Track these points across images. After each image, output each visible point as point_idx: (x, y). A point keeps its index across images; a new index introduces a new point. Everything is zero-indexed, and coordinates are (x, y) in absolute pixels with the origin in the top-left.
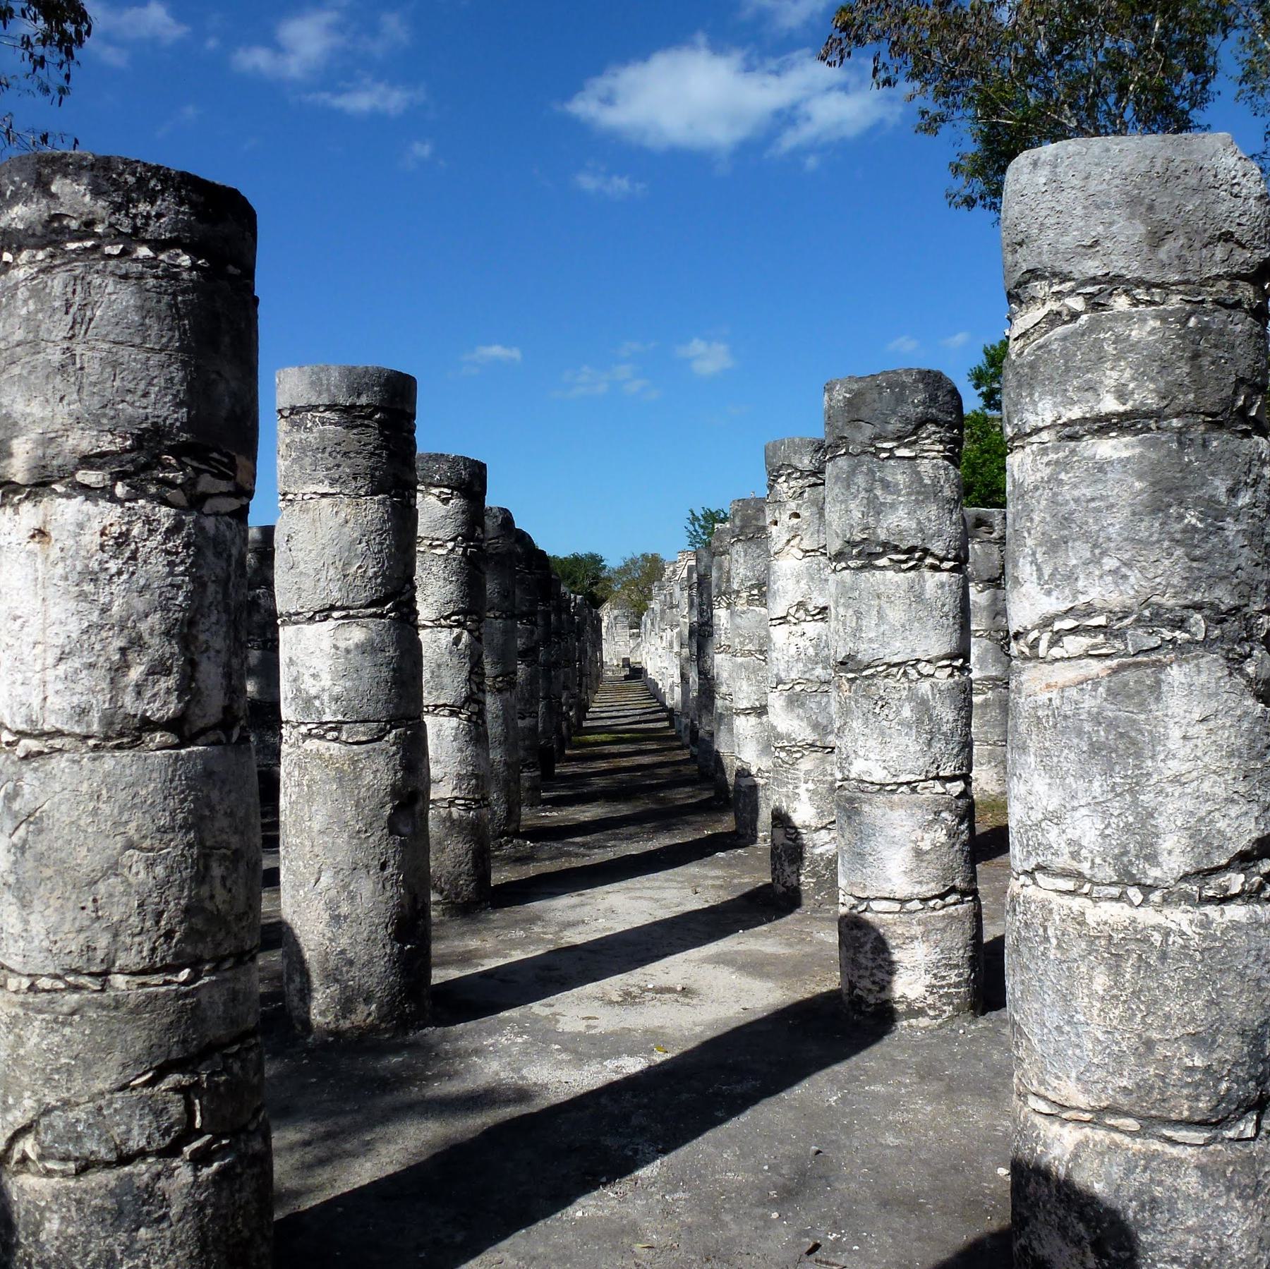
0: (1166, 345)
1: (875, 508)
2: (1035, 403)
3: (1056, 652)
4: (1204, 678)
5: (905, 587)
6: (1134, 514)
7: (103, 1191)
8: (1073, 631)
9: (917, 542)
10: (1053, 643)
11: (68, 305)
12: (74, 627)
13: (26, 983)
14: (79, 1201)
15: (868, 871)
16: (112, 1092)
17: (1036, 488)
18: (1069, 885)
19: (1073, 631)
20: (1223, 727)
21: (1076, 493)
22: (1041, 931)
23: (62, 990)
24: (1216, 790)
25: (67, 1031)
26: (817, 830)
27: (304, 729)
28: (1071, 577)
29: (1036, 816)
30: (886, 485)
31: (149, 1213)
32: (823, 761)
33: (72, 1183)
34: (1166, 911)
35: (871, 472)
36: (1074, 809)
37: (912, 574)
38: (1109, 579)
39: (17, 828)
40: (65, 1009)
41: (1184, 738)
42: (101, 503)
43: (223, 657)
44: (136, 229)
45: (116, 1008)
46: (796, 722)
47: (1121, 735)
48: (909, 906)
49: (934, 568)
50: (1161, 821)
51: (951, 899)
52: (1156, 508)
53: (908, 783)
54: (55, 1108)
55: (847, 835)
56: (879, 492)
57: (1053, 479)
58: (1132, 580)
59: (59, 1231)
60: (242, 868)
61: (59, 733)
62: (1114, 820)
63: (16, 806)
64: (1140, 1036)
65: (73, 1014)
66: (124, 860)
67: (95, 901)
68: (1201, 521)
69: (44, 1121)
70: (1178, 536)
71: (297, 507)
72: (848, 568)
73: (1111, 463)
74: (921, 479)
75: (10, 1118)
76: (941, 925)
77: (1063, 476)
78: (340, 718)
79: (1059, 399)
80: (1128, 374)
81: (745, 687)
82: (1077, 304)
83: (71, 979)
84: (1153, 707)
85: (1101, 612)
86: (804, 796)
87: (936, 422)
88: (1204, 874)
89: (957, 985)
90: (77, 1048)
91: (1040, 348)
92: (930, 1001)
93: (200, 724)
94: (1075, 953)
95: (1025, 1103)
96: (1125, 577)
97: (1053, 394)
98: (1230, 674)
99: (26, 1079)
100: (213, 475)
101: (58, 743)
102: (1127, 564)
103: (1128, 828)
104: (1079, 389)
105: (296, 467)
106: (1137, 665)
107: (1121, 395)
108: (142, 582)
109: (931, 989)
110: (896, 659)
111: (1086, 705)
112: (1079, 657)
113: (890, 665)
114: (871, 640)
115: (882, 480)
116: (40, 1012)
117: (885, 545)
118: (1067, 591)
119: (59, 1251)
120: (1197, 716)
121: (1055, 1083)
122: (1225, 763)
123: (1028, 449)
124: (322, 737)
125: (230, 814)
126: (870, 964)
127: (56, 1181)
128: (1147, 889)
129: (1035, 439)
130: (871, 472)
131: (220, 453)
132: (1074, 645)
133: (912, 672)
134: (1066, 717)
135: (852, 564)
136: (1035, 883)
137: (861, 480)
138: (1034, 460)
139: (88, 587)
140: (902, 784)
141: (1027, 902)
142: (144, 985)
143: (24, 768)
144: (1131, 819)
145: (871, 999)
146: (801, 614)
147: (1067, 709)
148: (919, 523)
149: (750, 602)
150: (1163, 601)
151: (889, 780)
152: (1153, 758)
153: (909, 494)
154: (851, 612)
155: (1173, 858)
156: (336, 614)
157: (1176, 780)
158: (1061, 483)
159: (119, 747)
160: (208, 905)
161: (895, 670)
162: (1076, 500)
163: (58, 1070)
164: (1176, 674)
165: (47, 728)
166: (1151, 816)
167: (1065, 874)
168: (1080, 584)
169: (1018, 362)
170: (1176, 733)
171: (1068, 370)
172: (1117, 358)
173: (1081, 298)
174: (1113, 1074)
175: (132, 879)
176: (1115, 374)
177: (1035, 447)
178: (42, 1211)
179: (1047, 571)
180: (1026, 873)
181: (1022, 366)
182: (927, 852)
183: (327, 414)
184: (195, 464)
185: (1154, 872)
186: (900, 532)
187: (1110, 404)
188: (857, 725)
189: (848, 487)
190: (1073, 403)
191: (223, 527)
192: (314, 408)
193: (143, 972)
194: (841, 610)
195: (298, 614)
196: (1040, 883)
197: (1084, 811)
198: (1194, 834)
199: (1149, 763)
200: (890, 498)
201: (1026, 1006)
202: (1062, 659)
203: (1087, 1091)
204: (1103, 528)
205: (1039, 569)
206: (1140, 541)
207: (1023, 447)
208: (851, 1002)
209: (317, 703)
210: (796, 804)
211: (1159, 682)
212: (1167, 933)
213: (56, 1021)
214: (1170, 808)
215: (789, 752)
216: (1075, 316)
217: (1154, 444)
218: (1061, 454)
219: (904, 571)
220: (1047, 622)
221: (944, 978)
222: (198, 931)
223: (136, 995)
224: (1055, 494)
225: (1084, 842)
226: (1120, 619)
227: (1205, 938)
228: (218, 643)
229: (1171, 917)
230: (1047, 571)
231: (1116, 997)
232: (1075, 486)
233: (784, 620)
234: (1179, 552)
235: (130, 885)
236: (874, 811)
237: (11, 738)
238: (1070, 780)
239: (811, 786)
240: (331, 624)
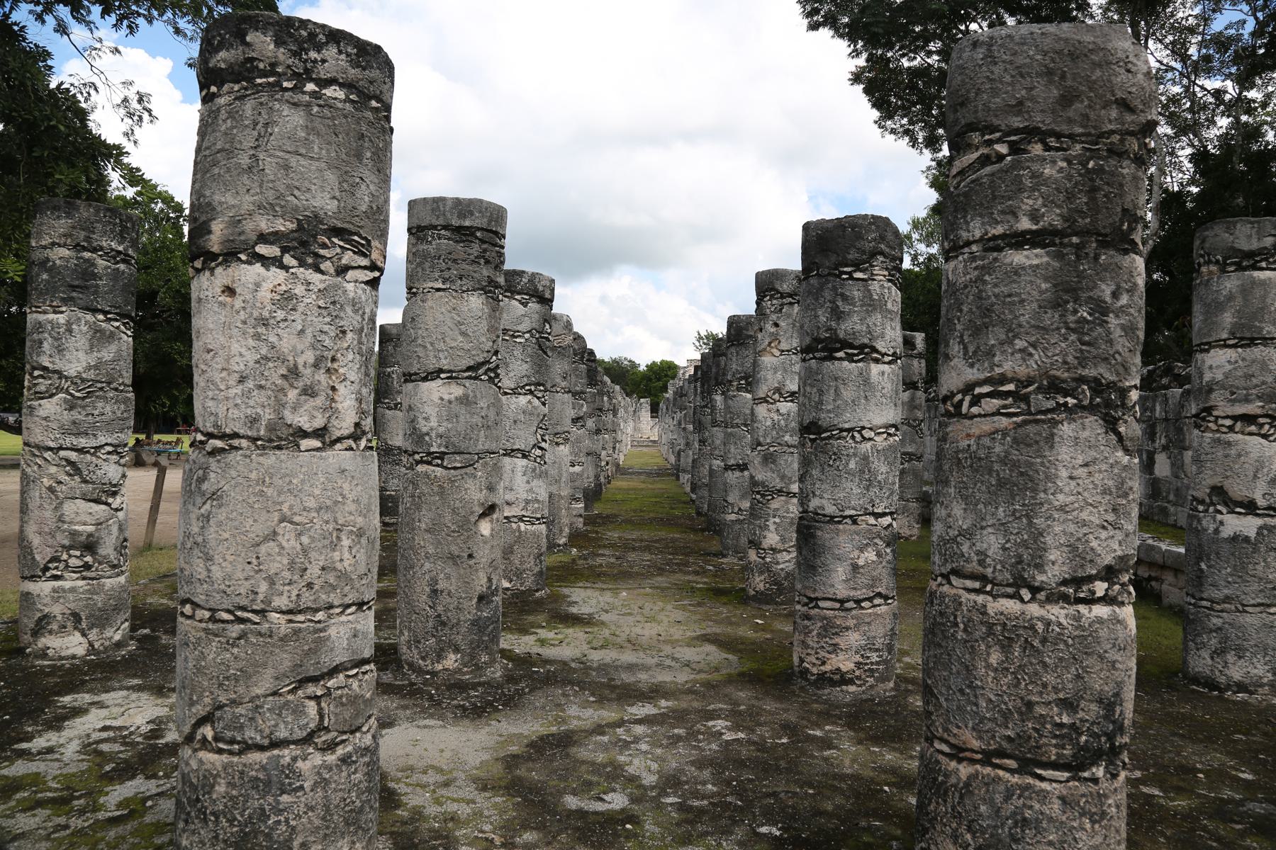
0: (1070, 181)
1: (838, 315)
2: (967, 223)
3: (975, 410)
4: (1086, 434)
5: (856, 373)
6: (1040, 307)
7: (257, 767)
8: (990, 395)
9: (866, 341)
10: (972, 404)
11: (256, 124)
12: (251, 357)
13: (207, 614)
14: (242, 773)
15: (818, 578)
16: (266, 696)
17: (966, 287)
18: (977, 585)
19: (990, 395)
21: (996, 290)
22: (952, 618)
23: (232, 621)
25: (235, 650)
26: (780, 551)
27: (417, 457)
28: (990, 354)
29: (953, 533)
30: (845, 298)
31: (290, 784)
32: (787, 502)
33: (236, 759)
34: (1048, 607)
35: (834, 289)
36: (982, 528)
37: (860, 364)
38: (1018, 356)
39: (204, 503)
40: (234, 635)
42: (273, 269)
43: (356, 387)
44: (307, 71)
45: (270, 636)
46: (769, 474)
47: (1022, 474)
48: (848, 605)
49: (877, 361)
50: (1049, 539)
51: (877, 601)
52: (1057, 304)
53: (851, 517)
54: (226, 705)
55: (804, 552)
56: (840, 303)
57: (979, 279)
58: (1037, 357)
59: (227, 793)
60: (364, 541)
61: (236, 435)
62: (1012, 537)
63: (205, 486)
64: (1022, 699)
65: (239, 639)
66: (280, 531)
67: (258, 558)
68: (1090, 314)
69: (218, 714)
70: (1072, 325)
71: (419, 298)
72: (814, 358)
73: (1023, 268)
75: (194, 710)
77: (987, 278)
78: (443, 449)
79: (986, 220)
80: (1040, 201)
81: (732, 450)
82: (1002, 149)
83: (239, 613)
84: (1047, 453)
85: (1010, 381)
86: (772, 527)
87: (882, 253)
88: (1077, 582)
89: (878, 663)
90: (241, 664)
91: (973, 182)
92: (857, 673)
93: (338, 434)
94: (977, 634)
95: (932, 745)
96: (1031, 355)
97: (981, 216)
98: (1106, 433)
99: (206, 683)
100: (354, 252)
101: (236, 442)
102: (1034, 346)
103: (1024, 544)
104: (1003, 212)
105: (419, 269)
106: (1037, 422)
107: (1034, 216)
108: (300, 327)
109: (858, 664)
110: (847, 426)
111: (997, 450)
112: (993, 414)
113: (842, 430)
114: (829, 411)
115: (842, 295)
116: (216, 635)
117: (840, 341)
118: (986, 365)
119: (226, 806)
120: (1080, 462)
121: (955, 731)
122: (1099, 498)
123: (960, 258)
124: (429, 463)
125: (356, 501)
126: (815, 645)
127: (225, 758)
128: (1035, 590)
129: (966, 250)
130: (834, 289)
131: (360, 236)
132: (992, 404)
133: (856, 434)
134: (980, 459)
135: (818, 355)
136: (949, 583)
137: (827, 294)
138: (965, 266)
139: (261, 330)
140: (845, 517)
141: (943, 596)
142: (290, 621)
143: (211, 460)
144: (1026, 537)
145: (815, 670)
146: (776, 396)
147: (982, 454)
149: (739, 389)
150: (1058, 373)
151: (838, 513)
152: (1045, 491)
153: (862, 306)
154: (815, 390)
155: (1056, 567)
156: (442, 376)
157: (1062, 509)
158: (985, 282)
159: (279, 448)
160: (339, 566)
161: (845, 434)
162: (996, 296)
163: (227, 678)
164: (1066, 429)
165: (228, 431)
166: (1041, 534)
167: (973, 577)
168: (996, 359)
169: (956, 192)
170: (1064, 473)
171: (994, 197)
172: (1033, 189)
173: (1005, 145)
174: (1000, 726)
175: (284, 544)
176: (1030, 202)
177: (966, 256)
178: (215, 777)
179: (971, 349)
180: (942, 575)
181: (958, 195)
182: (862, 567)
183: (443, 232)
184: (341, 243)
185: (1040, 578)
186: (854, 333)
187: (1025, 224)
188: (815, 473)
189: (817, 299)
190: (997, 223)
191: (360, 292)
192: (435, 227)
193: (290, 612)
194: (808, 389)
195: (416, 374)
196: (954, 583)
197: (990, 530)
198: (1073, 548)
199: (1042, 495)
200: (847, 308)
201: (936, 674)
202: (980, 415)
203: (981, 738)
204: (1016, 317)
205: (965, 348)
206: (1043, 328)
207: (957, 257)
208: (801, 672)
209: (427, 438)
210: (766, 533)
211: (1053, 435)
212: (1048, 623)
213: (228, 642)
214: (1057, 529)
215: (763, 496)
216: (1001, 157)
217: (1059, 256)
218: (986, 261)
219: (856, 362)
220: (968, 388)
221: (868, 658)
222: (331, 585)
223: (284, 629)
224: (981, 291)
225: (990, 553)
226: (1026, 387)
228: (353, 376)
229: (1053, 611)
230: (971, 349)
231: (1007, 669)
232: (996, 285)
233: (764, 400)
234: (1073, 337)
235: (283, 548)
236: (824, 534)
237: (203, 439)
238: (981, 506)
239: (777, 520)
240: (439, 382)
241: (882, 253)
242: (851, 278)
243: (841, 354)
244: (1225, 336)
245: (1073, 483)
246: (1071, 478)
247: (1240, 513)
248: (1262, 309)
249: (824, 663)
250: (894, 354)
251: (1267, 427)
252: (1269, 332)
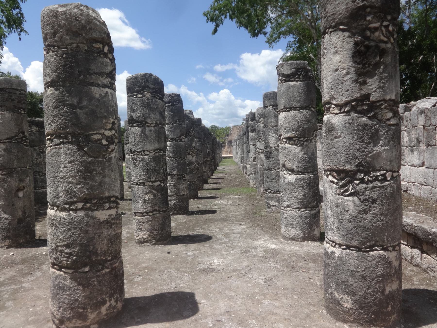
20: (76, 164)
24: (73, 181)
41: (65, 167)
49: (148, 126)
58: (53, 126)
96: (52, 125)
102: (52, 121)
106: (55, 148)
133: (142, 153)
206: (54, 116)
227: (70, 219)
242: (137, 97)
243: (135, 125)
244: (283, 108)
245: (66, 169)
246: (65, 167)
247: (290, 174)
248: (292, 96)
249: (138, 236)
250: (156, 123)
251: (297, 141)
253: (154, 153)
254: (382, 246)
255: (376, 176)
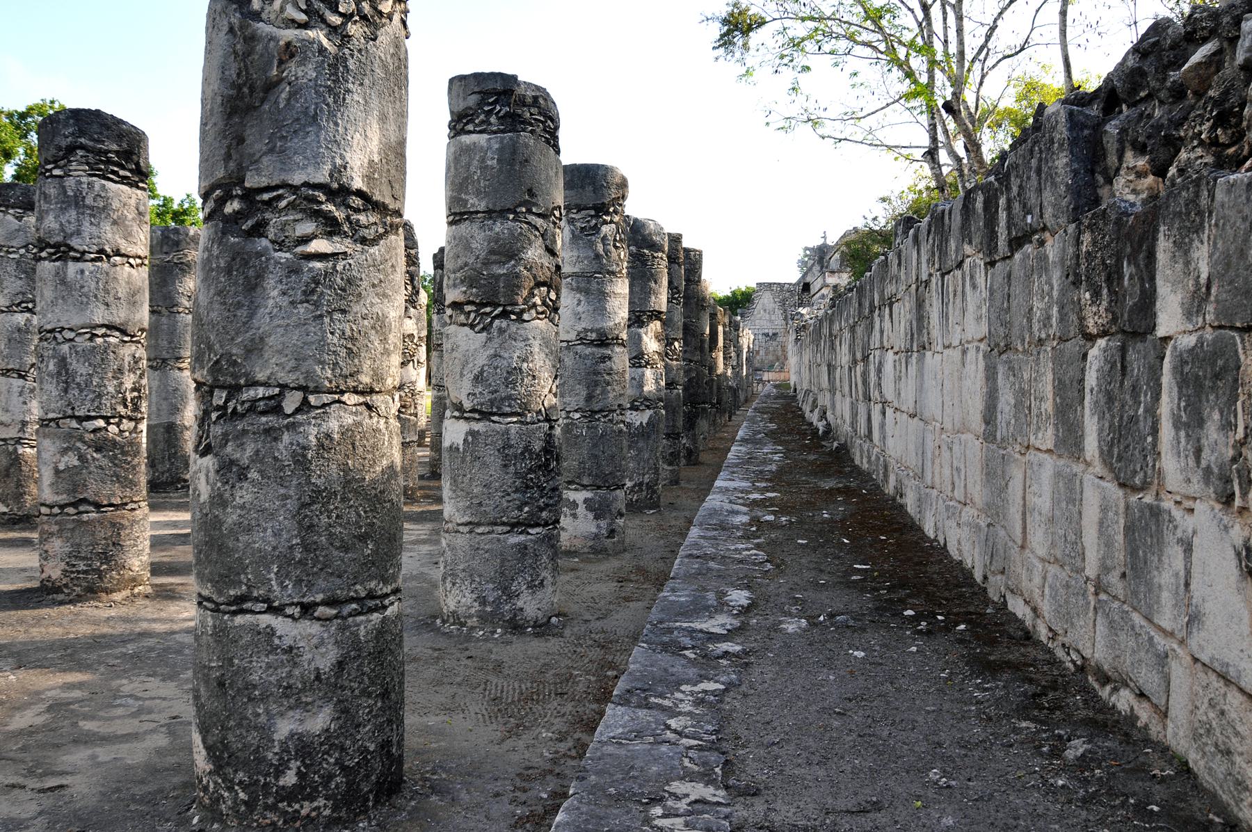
49: (76, 260)
74: (65, 192)
76: (70, 526)
133: (57, 335)
148: (61, 225)
241: (82, 147)
252: (473, 205)
253: (88, 336)
254: (267, 600)
255: (255, 401)
